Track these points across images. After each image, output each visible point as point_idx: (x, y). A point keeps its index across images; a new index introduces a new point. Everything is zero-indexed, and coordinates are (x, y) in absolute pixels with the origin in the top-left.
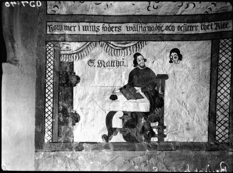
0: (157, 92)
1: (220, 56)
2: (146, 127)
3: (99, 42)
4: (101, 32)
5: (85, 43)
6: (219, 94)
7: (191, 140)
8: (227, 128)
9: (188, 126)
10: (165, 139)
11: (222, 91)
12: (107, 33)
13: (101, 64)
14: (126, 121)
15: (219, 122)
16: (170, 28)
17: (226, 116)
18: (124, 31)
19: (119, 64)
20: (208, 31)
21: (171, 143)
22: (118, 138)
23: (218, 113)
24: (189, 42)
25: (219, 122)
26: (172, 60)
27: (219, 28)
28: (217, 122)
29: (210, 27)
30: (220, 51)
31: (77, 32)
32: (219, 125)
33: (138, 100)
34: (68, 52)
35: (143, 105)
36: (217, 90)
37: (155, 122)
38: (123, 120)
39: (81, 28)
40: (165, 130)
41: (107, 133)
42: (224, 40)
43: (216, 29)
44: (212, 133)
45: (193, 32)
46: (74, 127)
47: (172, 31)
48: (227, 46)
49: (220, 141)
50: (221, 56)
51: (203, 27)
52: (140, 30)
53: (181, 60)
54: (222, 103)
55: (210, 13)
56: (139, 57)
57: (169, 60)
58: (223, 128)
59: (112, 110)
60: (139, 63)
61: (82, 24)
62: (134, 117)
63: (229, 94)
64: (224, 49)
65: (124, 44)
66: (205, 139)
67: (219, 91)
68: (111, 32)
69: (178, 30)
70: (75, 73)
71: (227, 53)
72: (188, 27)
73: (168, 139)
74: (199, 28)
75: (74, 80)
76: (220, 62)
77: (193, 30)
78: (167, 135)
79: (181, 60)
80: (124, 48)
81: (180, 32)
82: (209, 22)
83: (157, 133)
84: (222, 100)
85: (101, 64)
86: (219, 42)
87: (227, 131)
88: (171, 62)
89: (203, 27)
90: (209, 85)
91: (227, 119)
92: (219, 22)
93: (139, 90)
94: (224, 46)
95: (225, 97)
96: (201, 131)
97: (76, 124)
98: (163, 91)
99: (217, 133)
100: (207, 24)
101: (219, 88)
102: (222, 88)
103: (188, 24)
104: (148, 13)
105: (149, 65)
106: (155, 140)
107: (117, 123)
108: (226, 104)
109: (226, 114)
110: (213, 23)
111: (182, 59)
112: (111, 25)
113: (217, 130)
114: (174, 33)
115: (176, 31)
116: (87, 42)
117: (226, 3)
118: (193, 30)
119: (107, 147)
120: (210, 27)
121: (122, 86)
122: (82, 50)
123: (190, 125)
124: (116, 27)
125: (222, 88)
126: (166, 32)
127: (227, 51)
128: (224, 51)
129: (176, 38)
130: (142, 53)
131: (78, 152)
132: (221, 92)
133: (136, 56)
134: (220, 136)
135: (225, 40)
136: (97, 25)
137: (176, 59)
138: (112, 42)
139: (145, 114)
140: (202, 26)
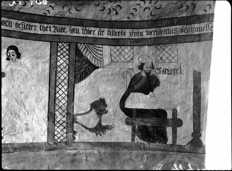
1: (58, 59)
6: (57, 95)
7: (31, 141)
9: (27, 126)
11: (61, 92)
15: (58, 122)
16: (7, 23)
17: (64, 116)
21: (9, 145)
23: (57, 113)
24: (28, 41)
25: (58, 122)
26: (10, 58)
27: (57, 31)
28: (56, 122)
29: (48, 29)
30: (59, 54)
32: (58, 125)
36: (55, 91)
42: (62, 44)
43: (54, 32)
44: (51, 133)
45: (32, 32)
47: (9, 27)
48: (65, 50)
49: (59, 140)
50: (59, 58)
51: (42, 28)
53: (20, 58)
54: (61, 104)
55: (48, 15)
57: (6, 57)
58: (61, 127)
63: (66, 95)
64: (62, 52)
66: (44, 139)
67: (58, 92)
69: (16, 27)
71: (64, 57)
72: (27, 25)
74: (38, 28)
76: (58, 64)
77: (32, 29)
78: (4, 137)
79: (20, 58)
81: (18, 29)
82: (48, 24)
84: (60, 101)
86: (58, 45)
87: (65, 131)
88: (8, 59)
89: (42, 28)
90: (48, 86)
91: (65, 119)
92: (58, 26)
94: (62, 49)
95: (63, 98)
96: (40, 131)
99: (56, 133)
100: (45, 25)
101: (57, 89)
102: (60, 89)
103: (27, 23)
108: (64, 104)
109: (64, 114)
110: (52, 26)
111: (21, 57)
113: (56, 130)
114: (11, 29)
115: (13, 28)
117: (120, 1)
118: (32, 29)
120: (48, 29)
123: (29, 125)
125: (60, 89)
127: (64, 54)
128: (62, 54)
129: (14, 35)
132: (59, 93)
134: (59, 135)
135: (63, 43)
137: (14, 57)
140: (40, 27)
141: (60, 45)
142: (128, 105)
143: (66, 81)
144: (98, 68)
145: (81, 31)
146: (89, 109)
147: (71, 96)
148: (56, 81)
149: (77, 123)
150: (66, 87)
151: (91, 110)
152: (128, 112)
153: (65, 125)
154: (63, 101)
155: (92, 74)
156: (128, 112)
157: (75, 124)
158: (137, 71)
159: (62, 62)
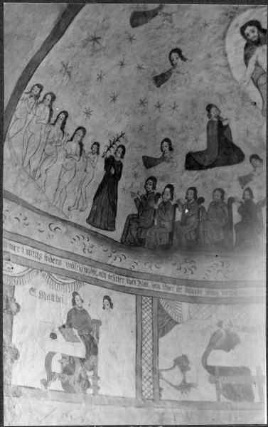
0: (92, 339)
2: (83, 376)
3: (41, 271)
4: (43, 261)
5: (25, 268)
8: (151, 383)
10: (100, 392)
11: (146, 345)
12: (48, 263)
13: (42, 295)
14: (64, 365)
18: (64, 266)
19: (59, 300)
20: (132, 286)
22: (56, 385)
25: (145, 377)
31: (20, 254)
32: (145, 380)
33: (75, 343)
34: (10, 274)
35: (79, 350)
37: (90, 370)
38: (62, 363)
39: (25, 251)
40: (99, 381)
41: (45, 376)
44: (139, 389)
46: (14, 365)
49: (146, 397)
50: (143, 311)
52: (78, 269)
56: (77, 297)
59: (52, 350)
60: (77, 303)
61: (25, 247)
62: (72, 362)
64: (146, 305)
65: (65, 279)
68: (52, 264)
70: (15, 300)
73: (102, 392)
75: (14, 307)
76: (144, 317)
80: (64, 284)
82: (133, 277)
83: (91, 384)
85: (42, 295)
87: (152, 386)
93: (75, 331)
97: (16, 361)
98: (98, 338)
100: (131, 279)
104: (82, 254)
105: (85, 307)
106: (90, 391)
107: (56, 368)
109: (150, 369)
112: (53, 257)
115: (107, 279)
116: (29, 267)
119: (45, 396)
121: (61, 325)
122: (24, 275)
124: (57, 260)
126: (99, 277)
130: (79, 292)
131: (15, 398)
133: (75, 294)
136: (40, 252)
138: (53, 275)
139: (82, 360)
141: (144, 298)
142: (210, 363)
143: (151, 334)
144: (177, 323)
145: (161, 287)
146: (172, 365)
147: (155, 350)
148: (142, 333)
149: (162, 379)
150: (151, 341)
151: (174, 366)
152: (211, 370)
153: (151, 380)
154: (149, 355)
155: (173, 330)
156: (211, 370)
157: (160, 380)
158: (216, 329)
159: (147, 315)
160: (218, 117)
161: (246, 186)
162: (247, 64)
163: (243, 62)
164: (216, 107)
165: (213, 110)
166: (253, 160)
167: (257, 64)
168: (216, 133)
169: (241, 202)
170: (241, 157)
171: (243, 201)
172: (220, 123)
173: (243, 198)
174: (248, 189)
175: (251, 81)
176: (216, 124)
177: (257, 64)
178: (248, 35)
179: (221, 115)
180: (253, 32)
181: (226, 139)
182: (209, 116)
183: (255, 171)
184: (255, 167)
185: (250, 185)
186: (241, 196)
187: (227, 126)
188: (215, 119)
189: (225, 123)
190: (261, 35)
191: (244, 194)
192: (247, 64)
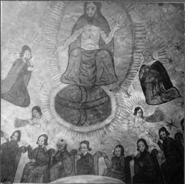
160: (27, 60)
161: (19, 129)
162: (73, 32)
163: (70, 29)
164: (30, 51)
165: (27, 52)
166: (35, 110)
167: (79, 38)
168: (18, 71)
169: (7, 140)
170: (26, 103)
171: (10, 140)
172: (26, 66)
173: (11, 137)
174: (19, 132)
175: (68, 49)
176: (23, 64)
177: (79, 38)
178: (88, 9)
179: (29, 61)
180: (93, 9)
181: (23, 82)
182: (22, 54)
183: (32, 119)
184: (33, 116)
185: (21, 129)
186: (11, 135)
187: (30, 72)
188: (25, 61)
189: (29, 69)
190: (96, 16)
191: (13, 134)
192: (73, 32)
